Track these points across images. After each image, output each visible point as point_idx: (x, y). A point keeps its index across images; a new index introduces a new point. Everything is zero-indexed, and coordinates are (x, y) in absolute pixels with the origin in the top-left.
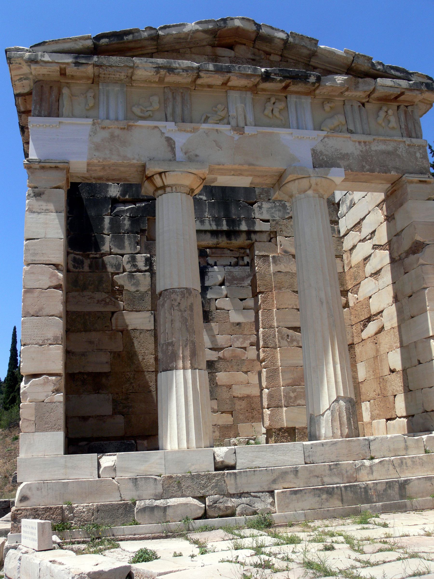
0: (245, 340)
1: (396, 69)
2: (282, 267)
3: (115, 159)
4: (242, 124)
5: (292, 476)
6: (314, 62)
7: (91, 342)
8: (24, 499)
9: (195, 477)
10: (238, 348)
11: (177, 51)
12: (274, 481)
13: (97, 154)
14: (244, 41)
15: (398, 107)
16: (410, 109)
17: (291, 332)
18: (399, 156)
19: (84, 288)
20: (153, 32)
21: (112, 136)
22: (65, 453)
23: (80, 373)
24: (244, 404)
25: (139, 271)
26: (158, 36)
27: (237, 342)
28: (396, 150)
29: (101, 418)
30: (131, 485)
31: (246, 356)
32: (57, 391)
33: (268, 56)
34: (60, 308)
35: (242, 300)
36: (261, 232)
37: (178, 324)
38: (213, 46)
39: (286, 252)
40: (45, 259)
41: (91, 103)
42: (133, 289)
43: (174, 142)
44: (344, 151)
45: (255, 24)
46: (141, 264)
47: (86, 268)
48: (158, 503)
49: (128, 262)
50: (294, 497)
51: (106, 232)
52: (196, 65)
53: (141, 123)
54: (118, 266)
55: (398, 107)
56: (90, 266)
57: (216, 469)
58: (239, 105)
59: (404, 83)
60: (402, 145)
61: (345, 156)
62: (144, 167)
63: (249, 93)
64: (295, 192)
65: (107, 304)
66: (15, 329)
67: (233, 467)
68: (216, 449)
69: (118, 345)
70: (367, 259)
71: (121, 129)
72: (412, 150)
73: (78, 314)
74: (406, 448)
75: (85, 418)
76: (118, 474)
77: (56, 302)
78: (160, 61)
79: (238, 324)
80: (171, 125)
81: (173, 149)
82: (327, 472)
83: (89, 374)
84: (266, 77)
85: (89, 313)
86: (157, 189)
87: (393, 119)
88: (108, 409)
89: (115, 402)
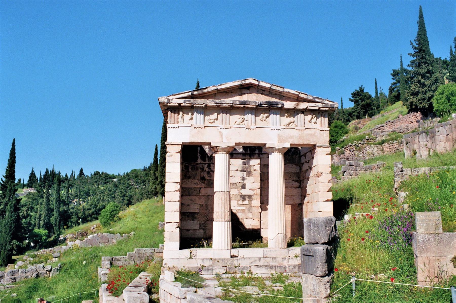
4: (250, 124)
5: (258, 261)
6: (282, 94)
7: (191, 200)
8: (166, 264)
9: (223, 260)
11: (226, 92)
12: (252, 263)
15: (319, 113)
16: (324, 114)
19: (189, 178)
20: (215, 88)
23: (187, 212)
26: (217, 89)
28: (315, 133)
29: (195, 230)
30: (201, 261)
32: (177, 228)
33: (264, 92)
37: (220, 205)
38: (241, 89)
42: (209, 178)
47: (190, 170)
49: (207, 167)
50: (258, 269)
51: (198, 154)
52: (231, 102)
54: (203, 169)
55: (319, 113)
56: (192, 169)
57: (231, 257)
59: (320, 105)
61: (292, 137)
63: (254, 110)
64: (270, 152)
65: (198, 185)
66: (157, 146)
67: (237, 257)
68: (232, 250)
69: (202, 201)
70: (307, 170)
73: (186, 188)
75: (188, 230)
76: (197, 257)
78: (218, 101)
81: (222, 136)
82: (272, 261)
83: (190, 213)
85: (191, 188)
88: (197, 227)
89: (200, 224)
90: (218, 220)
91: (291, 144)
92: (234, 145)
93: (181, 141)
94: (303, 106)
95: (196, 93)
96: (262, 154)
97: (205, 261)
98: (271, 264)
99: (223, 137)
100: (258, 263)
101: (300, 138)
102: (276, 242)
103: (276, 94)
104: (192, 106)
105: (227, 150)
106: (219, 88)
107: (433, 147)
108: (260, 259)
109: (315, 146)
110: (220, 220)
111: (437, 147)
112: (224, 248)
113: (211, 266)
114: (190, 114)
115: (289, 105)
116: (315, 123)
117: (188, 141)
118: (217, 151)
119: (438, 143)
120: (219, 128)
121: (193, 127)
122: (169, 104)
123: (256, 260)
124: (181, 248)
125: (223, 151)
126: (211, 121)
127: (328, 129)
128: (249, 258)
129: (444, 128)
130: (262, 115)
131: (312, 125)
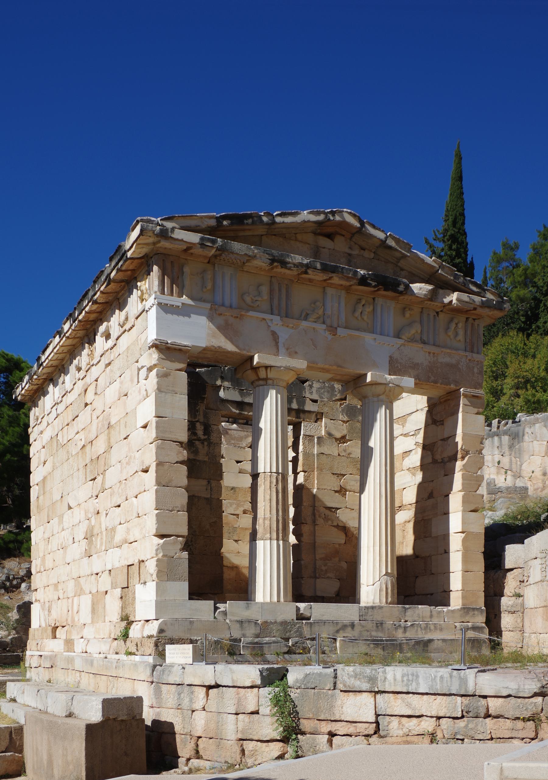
0: (238, 506)
10: (232, 514)
13: (214, 340)
27: (231, 508)
31: (238, 524)
43: (278, 336)
99: (281, 345)
107: (514, 466)
111: (524, 467)
117: (203, 343)
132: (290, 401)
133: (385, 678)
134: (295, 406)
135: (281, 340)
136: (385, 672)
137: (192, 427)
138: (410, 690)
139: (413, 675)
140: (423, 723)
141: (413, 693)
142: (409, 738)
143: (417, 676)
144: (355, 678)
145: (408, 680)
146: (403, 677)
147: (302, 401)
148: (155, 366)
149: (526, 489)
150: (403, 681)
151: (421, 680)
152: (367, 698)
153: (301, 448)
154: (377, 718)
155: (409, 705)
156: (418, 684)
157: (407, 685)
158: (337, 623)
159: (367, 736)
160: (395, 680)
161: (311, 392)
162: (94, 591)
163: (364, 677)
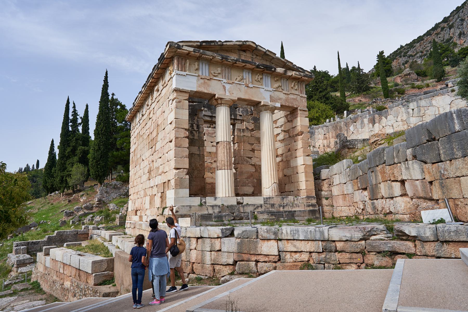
0: (212, 159)
1: (301, 68)
2: (246, 134)
3: (206, 91)
4: (248, 83)
9: (232, 206)
12: (255, 209)
14: (250, 50)
16: (302, 83)
17: (247, 159)
18: (297, 100)
21: (205, 82)
22: (190, 196)
24: (210, 186)
25: (195, 131)
26: (223, 45)
32: (187, 174)
34: (187, 145)
35: (211, 142)
36: (239, 120)
37: (226, 154)
39: (247, 128)
40: (182, 127)
41: (197, 67)
42: (192, 137)
44: (280, 97)
45: (256, 45)
46: (195, 128)
48: (220, 214)
53: (215, 78)
58: (247, 76)
59: (302, 74)
60: (299, 97)
61: (280, 99)
62: (215, 95)
67: (242, 204)
71: (208, 80)
72: (302, 98)
74: (294, 201)
76: (207, 204)
77: (186, 143)
79: (210, 152)
80: (225, 81)
81: (225, 90)
84: (258, 67)
86: (218, 104)
87: (296, 86)
90: (223, 168)
91: (281, 106)
92: (237, 99)
93: (189, 89)
94: (290, 73)
95: (204, 44)
96: (237, 120)
97: (215, 207)
98: (270, 209)
100: (260, 209)
101: (286, 100)
102: (272, 190)
103: (267, 60)
104: (200, 57)
105: (229, 103)
106: (224, 44)
108: (261, 206)
109: (297, 108)
110: (226, 168)
112: (230, 196)
113: (220, 212)
114: (196, 64)
115: (280, 70)
116: (296, 90)
117: (195, 90)
118: (221, 104)
119: (317, 140)
120: (222, 82)
121: (200, 78)
122: (178, 50)
123: (258, 207)
124: (191, 195)
125: (226, 104)
126: (216, 75)
127: (306, 96)
128: (253, 205)
129: (323, 129)
130: (257, 76)
131: (293, 92)
132: (231, 116)
133: (282, 232)
134: (233, 117)
135: (227, 89)
136: (282, 229)
137: (192, 126)
138: (295, 238)
139: (296, 230)
140: (302, 255)
141: (297, 240)
142: (296, 264)
143: (298, 231)
144: (267, 232)
145: (294, 233)
146: (291, 232)
147: (235, 115)
148: (175, 98)
149: (318, 152)
150: (291, 234)
151: (300, 233)
152: (273, 243)
153: (236, 134)
154: (279, 253)
155: (295, 246)
156: (299, 235)
157: (293, 236)
158: (255, 205)
159: (275, 262)
160: (287, 233)
161: (239, 112)
162: (151, 195)
163: (272, 232)
